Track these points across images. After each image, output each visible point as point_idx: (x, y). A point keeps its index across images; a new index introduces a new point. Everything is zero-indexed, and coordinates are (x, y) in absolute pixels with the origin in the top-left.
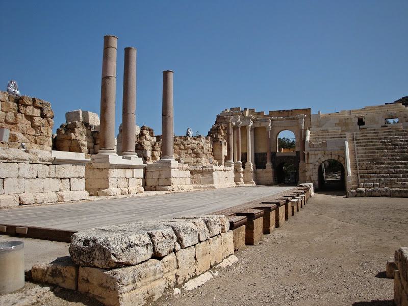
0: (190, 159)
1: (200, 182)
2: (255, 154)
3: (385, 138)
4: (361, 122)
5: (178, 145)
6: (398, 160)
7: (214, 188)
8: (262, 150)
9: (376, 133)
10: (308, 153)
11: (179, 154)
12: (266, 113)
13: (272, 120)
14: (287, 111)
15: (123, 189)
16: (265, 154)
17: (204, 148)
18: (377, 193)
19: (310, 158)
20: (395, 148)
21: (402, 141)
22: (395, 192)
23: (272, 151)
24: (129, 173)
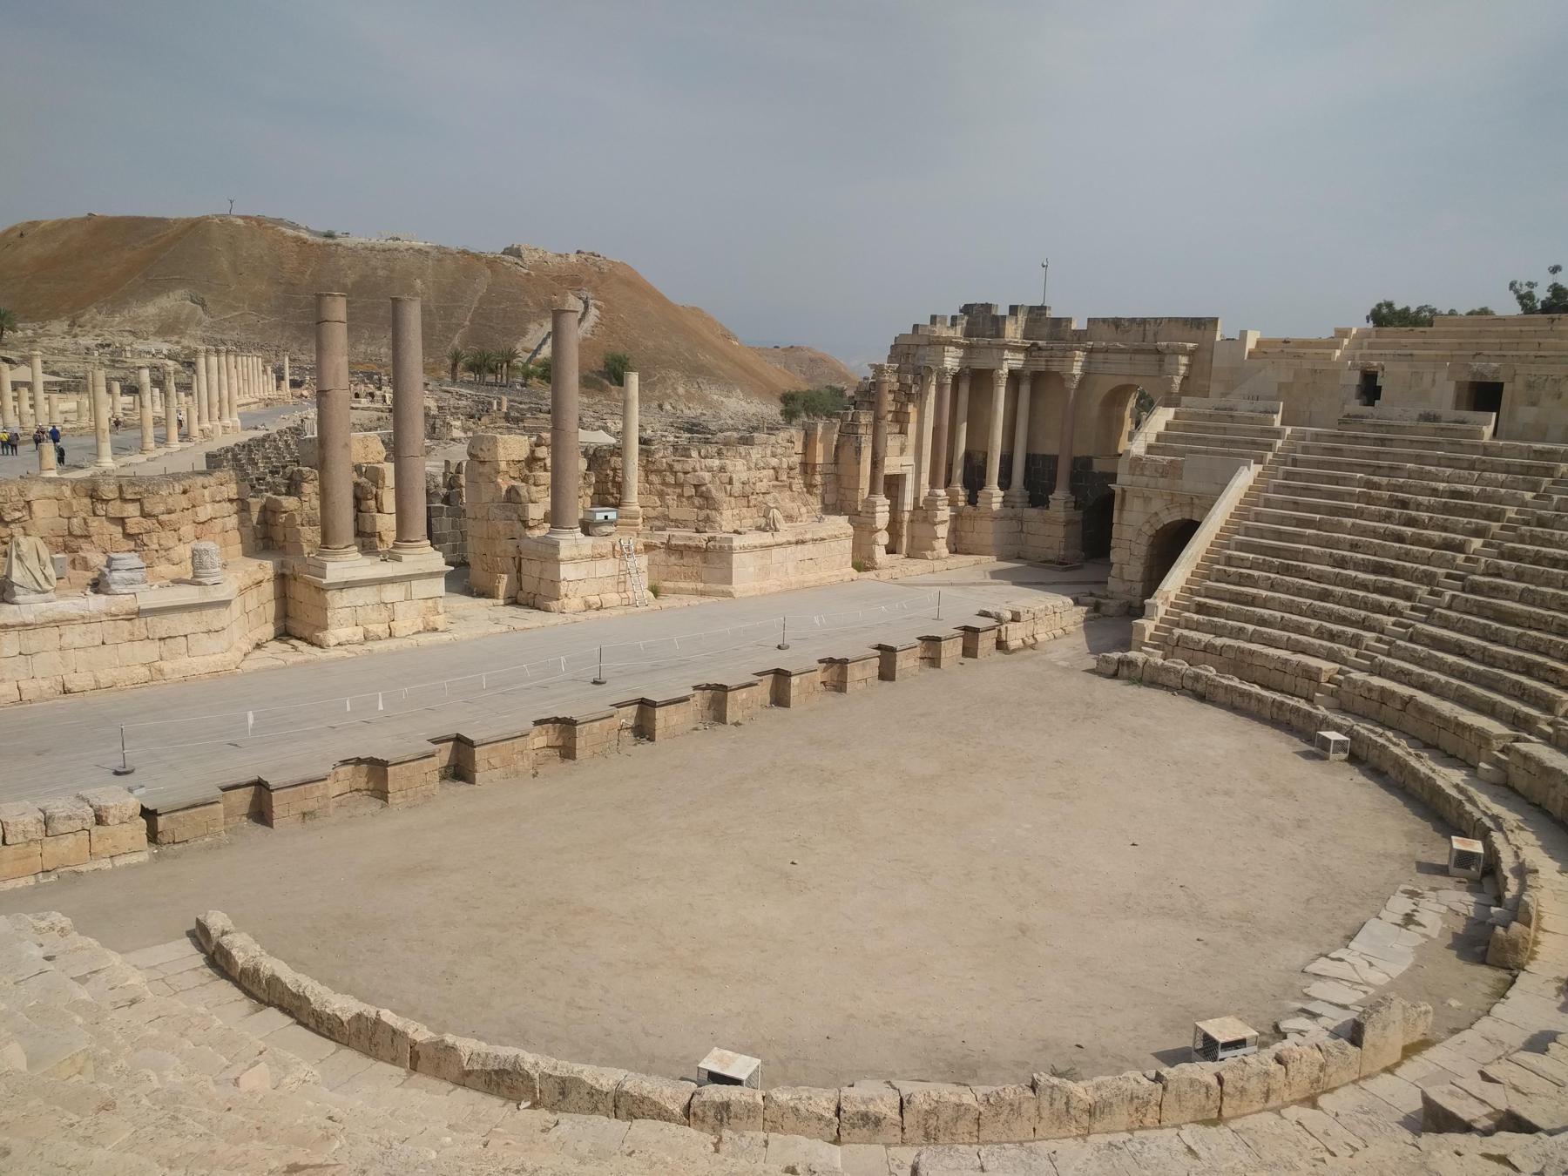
0: (686, 512)
1: (699, 577)
2: (1030, 459)
3: (1391, 468)
4: (1370, 389)
5: (658, 472)
6: (1358, 566)
7: (730, 595)
8: (1048, 447)
9: (1382, 442)
10: (1124, 491)
11: (661, 495)
12: (1079, 324)
13: (1091, 351)
14: (1144, 321)
15: (370, 627)
16: (1054, 459)
17: (737, 485)
18: (1173, 680)
19: (1127, 507)
20: (1387, 518)
21: (1435, 492)
22: (1216, 687)
23: (1080, 450)
24: (392, 593)
